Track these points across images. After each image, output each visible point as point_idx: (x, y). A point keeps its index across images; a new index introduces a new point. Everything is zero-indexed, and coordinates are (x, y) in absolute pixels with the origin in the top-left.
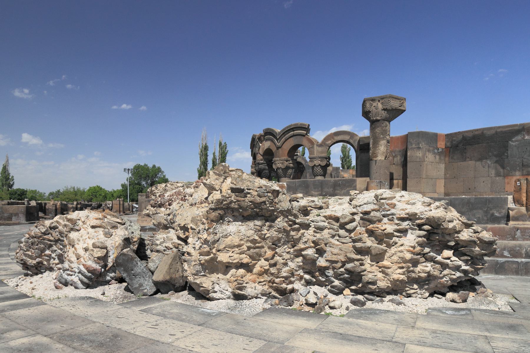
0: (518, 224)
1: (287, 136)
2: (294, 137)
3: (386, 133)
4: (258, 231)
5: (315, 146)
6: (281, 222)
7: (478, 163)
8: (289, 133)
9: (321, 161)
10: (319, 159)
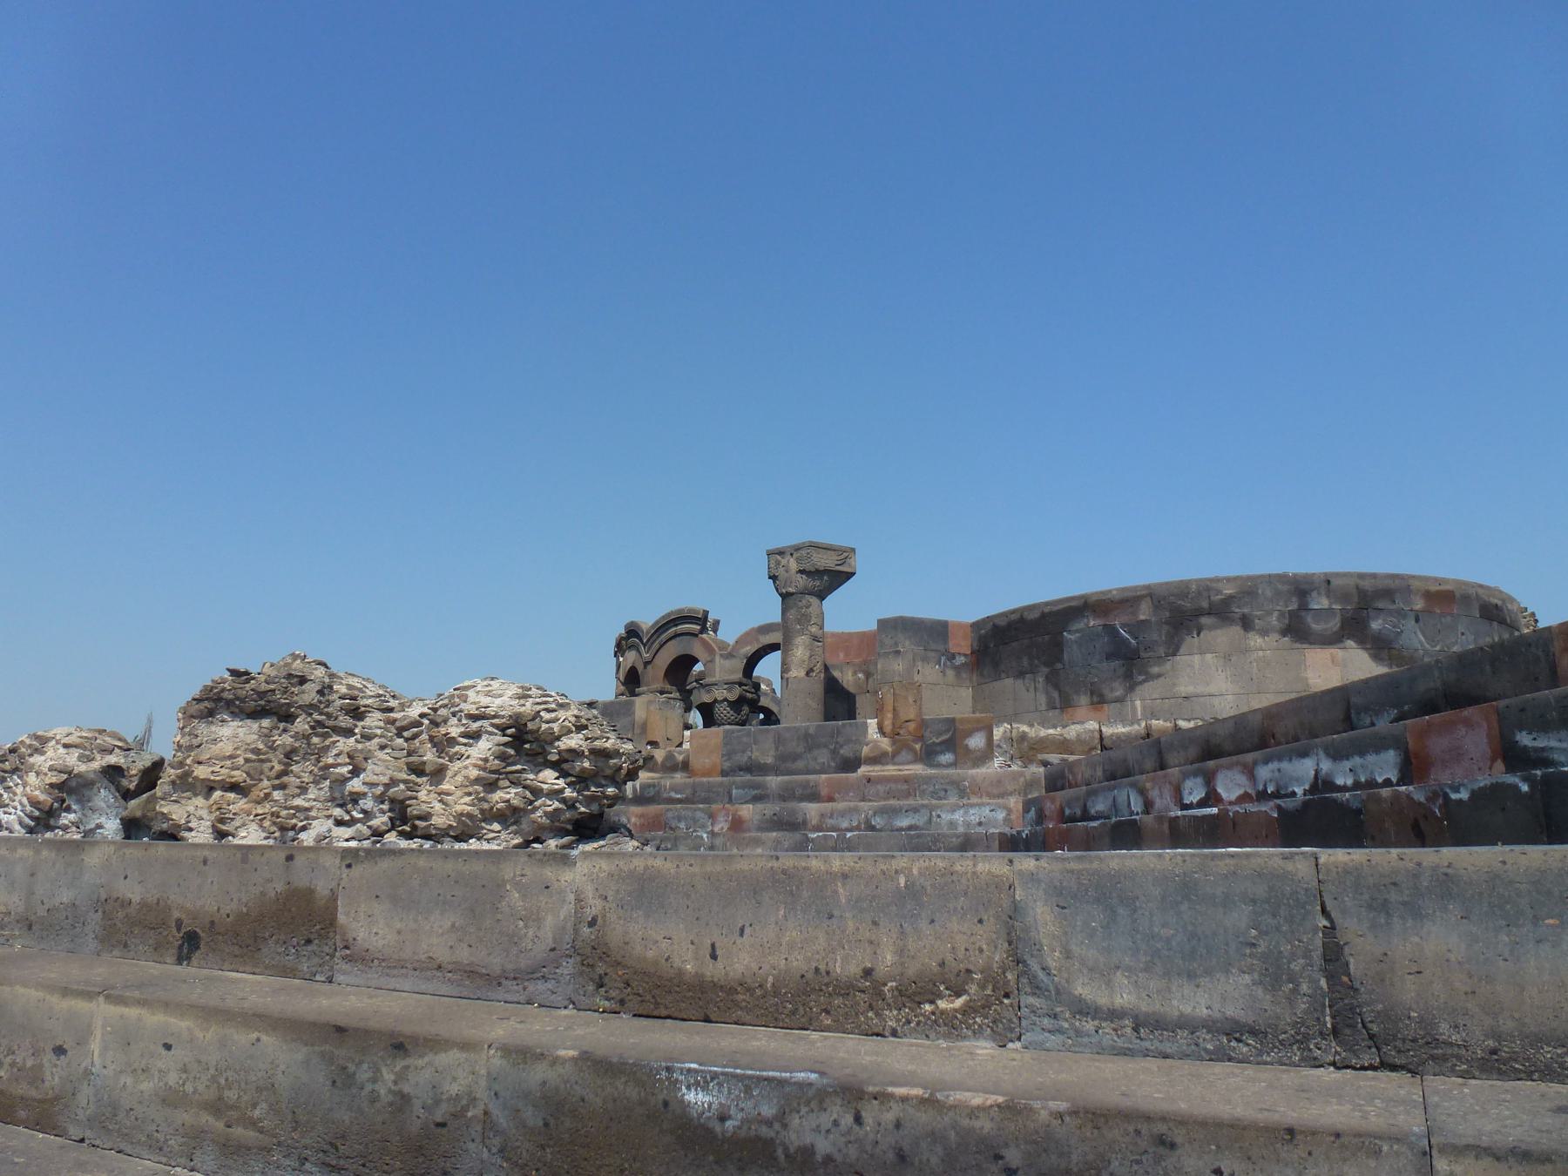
0: (873, 771)
1: (664, 636)
2: (678, 638)
3: (810, 621)
4: (266, 736)
5: (717, 658)
6: (301, 724)
7: (1019, 682)
8: (667, 630)
9: (729, 690)
10: (726, 686)
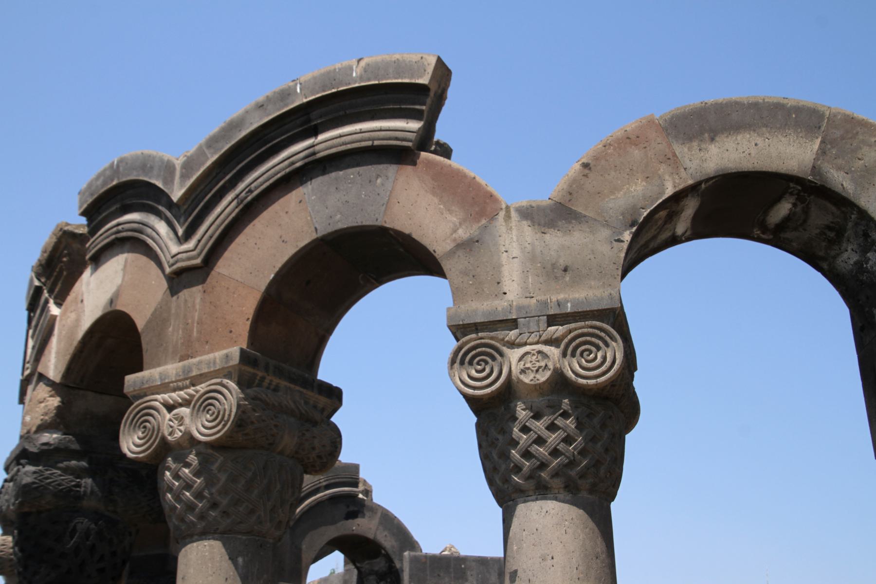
10: (557, 330)
